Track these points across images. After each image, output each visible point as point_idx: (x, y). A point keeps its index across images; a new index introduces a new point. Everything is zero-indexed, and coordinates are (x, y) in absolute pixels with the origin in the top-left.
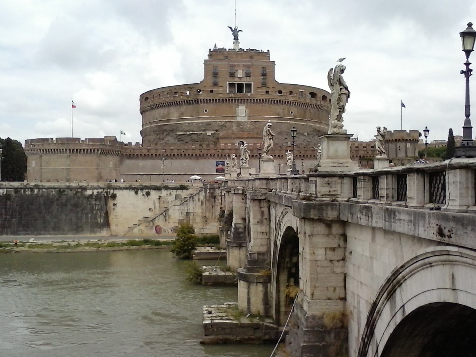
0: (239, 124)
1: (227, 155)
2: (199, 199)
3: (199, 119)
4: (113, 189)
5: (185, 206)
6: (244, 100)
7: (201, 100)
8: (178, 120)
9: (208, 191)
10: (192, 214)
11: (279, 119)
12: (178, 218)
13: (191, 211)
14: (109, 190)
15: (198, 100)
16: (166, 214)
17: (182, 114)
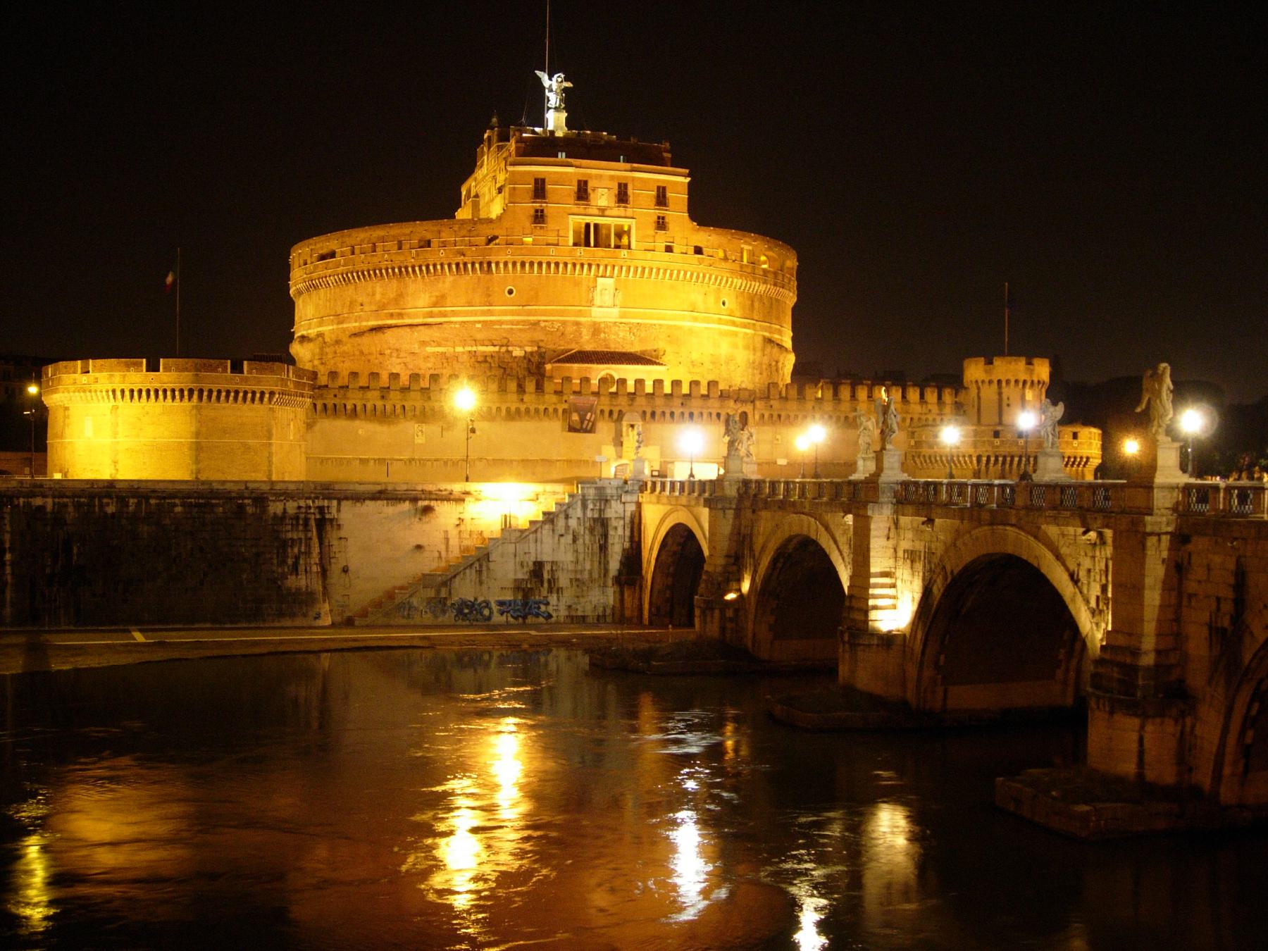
0: (596, 329)
2: (567, 527)
3: (490, 313)
4: (339, 500)
5: (532, 545)
7: (497, 264)
8: (431, 315)
9: (591, 506)
10: (547, 567)
11: (695, 319)
12: (511, 576)
13: (545, 559)
14: (326, 503)
15: (489, 264)
16: (481, 566)
17: (440, 301)
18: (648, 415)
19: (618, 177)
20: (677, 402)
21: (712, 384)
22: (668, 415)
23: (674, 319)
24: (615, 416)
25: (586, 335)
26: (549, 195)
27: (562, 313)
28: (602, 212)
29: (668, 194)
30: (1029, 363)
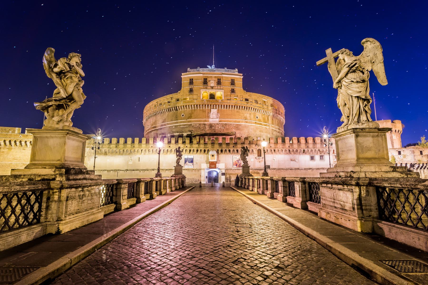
0: (211, 126)
1: (195, 150)
3: (177, 123)
6: (216, 105)
8: (162, 126)
15: (176, 107)
18: (220, 152)
19: (218, 77)
20: (231, 146)
21: (246, 138)
22: (228, 151)
23: (239, 122)
24: (206, 152)
25: (207, 128)
26: (194, 83)
27: (200, 121)
28: (212, 88)
29: (235, 82)
30: (392, 122)
